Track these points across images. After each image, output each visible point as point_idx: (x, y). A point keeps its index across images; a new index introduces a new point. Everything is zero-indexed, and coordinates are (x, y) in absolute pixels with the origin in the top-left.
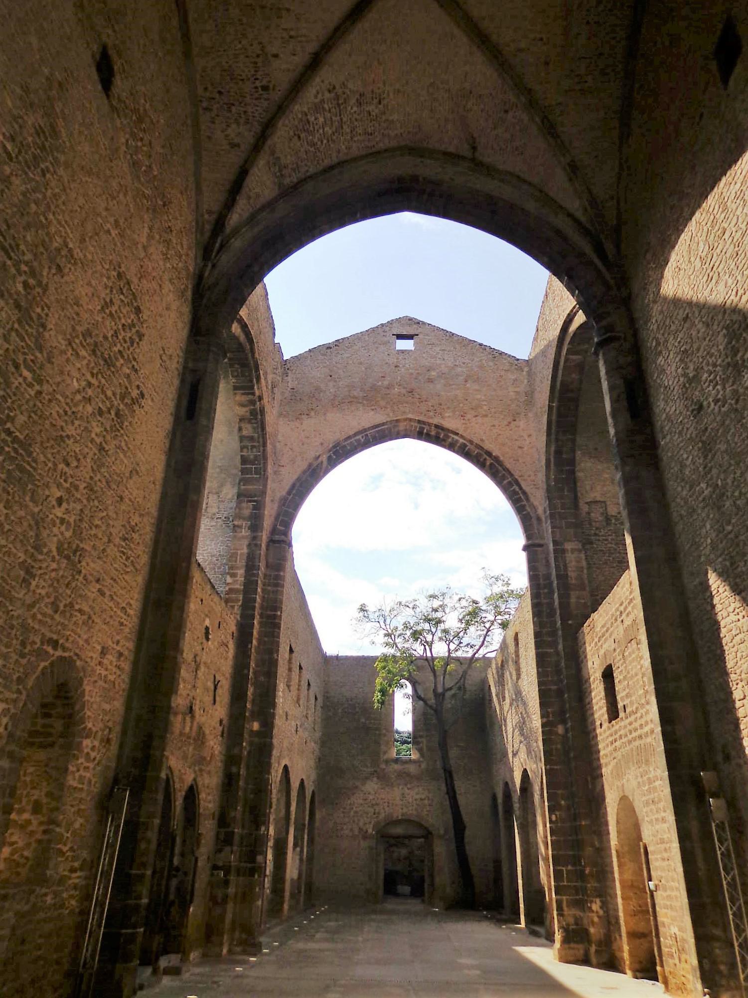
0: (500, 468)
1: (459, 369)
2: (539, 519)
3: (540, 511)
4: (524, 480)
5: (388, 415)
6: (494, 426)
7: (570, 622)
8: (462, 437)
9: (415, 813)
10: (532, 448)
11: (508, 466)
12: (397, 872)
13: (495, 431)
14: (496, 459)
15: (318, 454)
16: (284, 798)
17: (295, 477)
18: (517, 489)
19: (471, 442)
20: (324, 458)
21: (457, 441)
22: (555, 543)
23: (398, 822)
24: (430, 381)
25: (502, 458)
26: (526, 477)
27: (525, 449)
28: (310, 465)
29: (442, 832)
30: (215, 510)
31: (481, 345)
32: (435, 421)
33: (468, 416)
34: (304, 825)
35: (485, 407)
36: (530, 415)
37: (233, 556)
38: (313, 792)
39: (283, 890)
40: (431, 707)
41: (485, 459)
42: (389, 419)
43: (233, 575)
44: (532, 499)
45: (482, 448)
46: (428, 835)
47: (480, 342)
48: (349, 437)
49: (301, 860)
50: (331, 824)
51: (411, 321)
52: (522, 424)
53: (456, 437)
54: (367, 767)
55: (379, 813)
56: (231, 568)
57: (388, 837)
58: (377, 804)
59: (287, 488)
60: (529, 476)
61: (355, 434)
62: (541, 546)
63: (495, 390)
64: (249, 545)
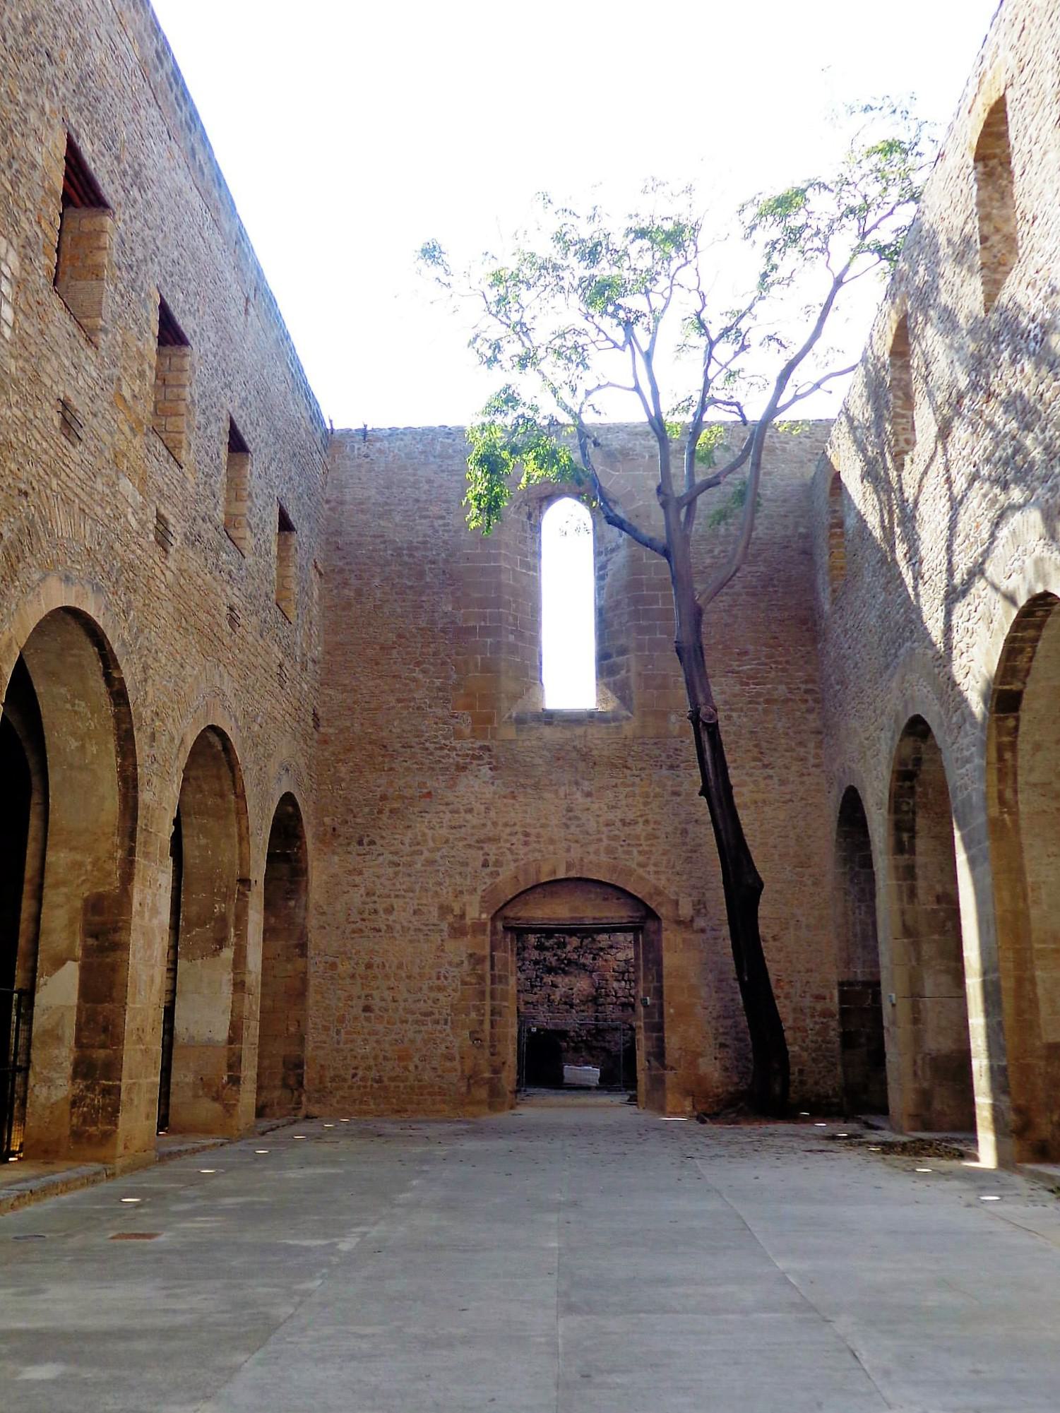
9: (604, 858)
12: (563, 1034)
16: (113, 760)
23: (554, 886)
29: (686, 910)
34: (245, 882)
38: (288, 799)
39: (112, 1068)
40: (649, 544)
46: (643, 919)
49: (239, 986)
50: (357, 897)
54: (458, 735)
55: (498, 863)
57: (527, 931)
58: (490, 840)
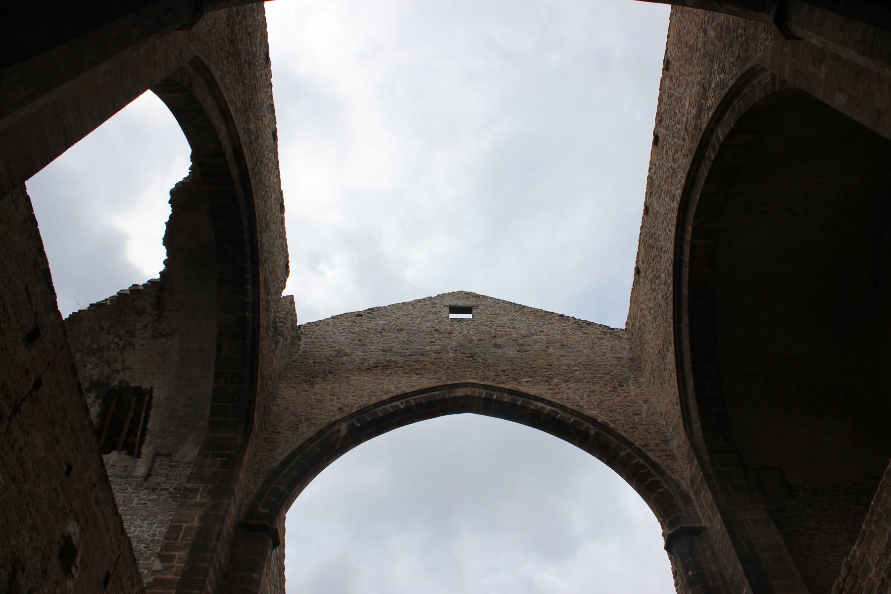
0: (611, 438)
3: (685, 485)
4: (651, 450)
6: (594, 391)
8: (549, 403)
11: (623, 434)
13: (596, 397)
14: (604, 426)
15: (333, 419)
17: (296, 445)
18: (642, 462)
19: (563, 408)
20: (344, 428)
21: (542, 407)
24: (496, 346)
25: (612, 425)
27: (644, 415)
28: (320, 433)
30: (159, 479)
32: (508, 386)
33: (555, 381)
36: (642, 380)
37: (173, 531)
42: (440, 384)
43: (165, 558)
44: (668, 472)
45: (581, 415)
48: (383, 403)
51: (468, 295)
52: (633, 390)
53: (540, 404)
56: (165, 548)
59: (282, 458)
60: (657, 445)
63: (588, 356)
64: (203, 518)
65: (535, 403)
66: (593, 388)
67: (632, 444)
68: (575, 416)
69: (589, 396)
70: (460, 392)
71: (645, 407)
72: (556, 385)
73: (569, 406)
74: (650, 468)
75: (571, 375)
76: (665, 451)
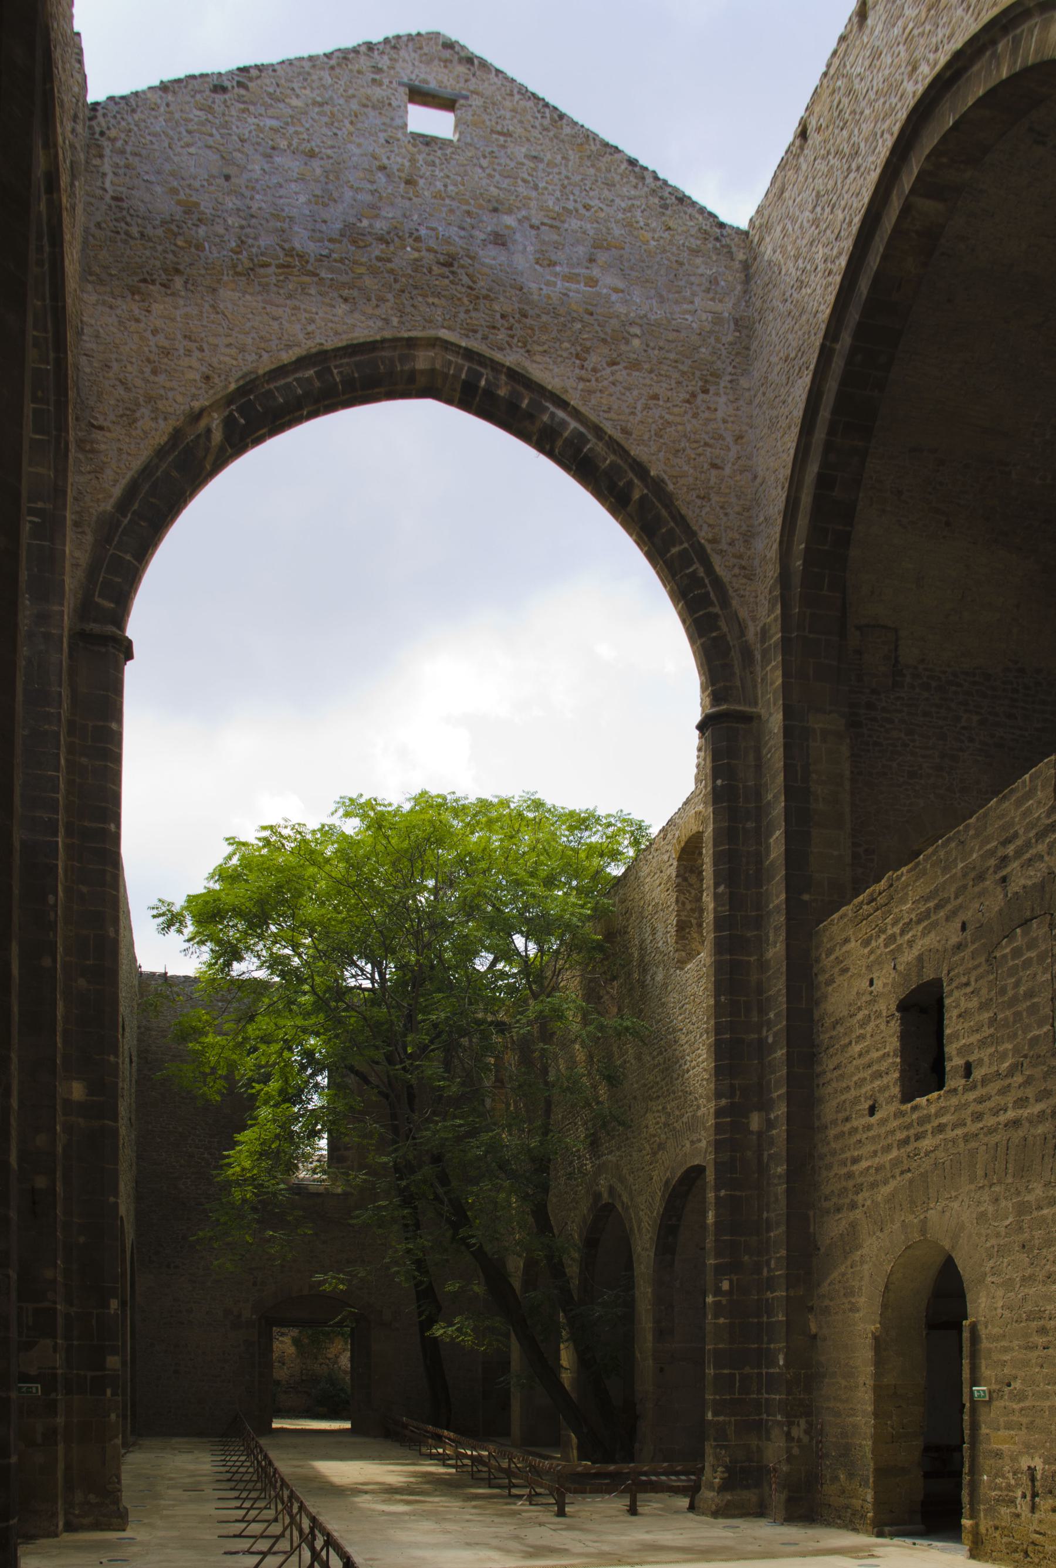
0: (664, 513)
1: (574, 224)
2: (747, 654)
4: (721, 552)
5: (387, 321)
6: (656, 397)
7: (806, 897)
8: (576, 414)
10: (741, 472)
14: (657, 486)
18: (701, 573)
19: (598, 431)
21: (564, 424)
22: (788, 712)
26: (724, 546)
31: (632, 162)
32: (510, 359)
33: (593, 359)
35: (636, 342)
41: (630, 483)
42: (388, 334)
44: (734, 603)
45: (621, 451)
47: (632, 153)
53: (561, 414)
60: (731, 543)
61: (301, 363)
62: (748, 718)
65: (552, 409)
66: (656, 389)
67: (694, 534)
68: (615, 452)
69: (647, 407)
70: (423, 360)
71: (734, 449)
72: (595, 370)
73: (608, 428)
74: (709, 588)
75: (623, 347)
76: (740, 557)
